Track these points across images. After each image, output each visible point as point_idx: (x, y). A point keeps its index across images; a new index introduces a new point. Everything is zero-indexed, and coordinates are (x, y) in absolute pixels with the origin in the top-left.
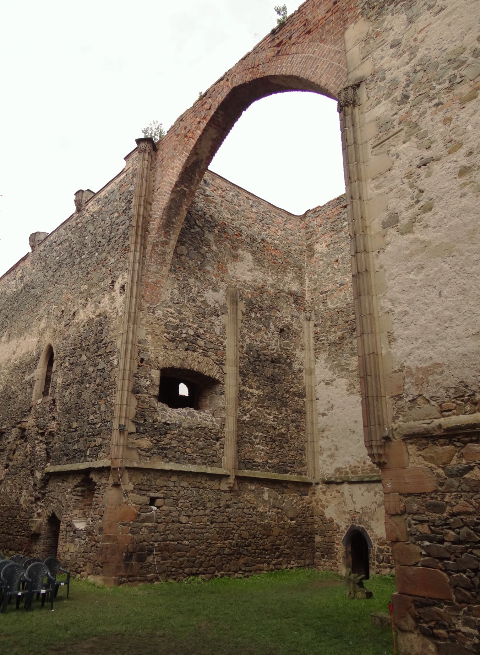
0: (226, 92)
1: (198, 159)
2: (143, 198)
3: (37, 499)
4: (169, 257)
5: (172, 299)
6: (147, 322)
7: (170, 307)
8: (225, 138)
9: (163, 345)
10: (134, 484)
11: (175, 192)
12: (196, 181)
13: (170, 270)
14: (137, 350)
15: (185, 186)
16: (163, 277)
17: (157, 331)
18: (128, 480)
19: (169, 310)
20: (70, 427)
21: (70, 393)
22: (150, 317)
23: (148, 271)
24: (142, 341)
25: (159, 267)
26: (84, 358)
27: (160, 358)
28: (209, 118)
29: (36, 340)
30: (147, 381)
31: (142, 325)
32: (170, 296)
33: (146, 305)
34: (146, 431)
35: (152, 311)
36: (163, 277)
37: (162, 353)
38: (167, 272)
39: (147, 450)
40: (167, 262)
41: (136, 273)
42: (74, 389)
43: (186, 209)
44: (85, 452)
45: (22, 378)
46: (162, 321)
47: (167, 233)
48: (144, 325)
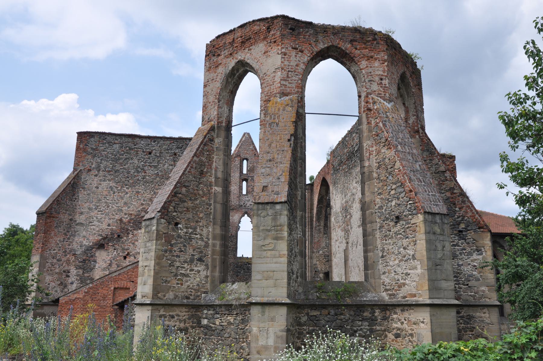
4: (322, 230)
7: (325, 248)
16: (321, 238)
19: (325, 250)
22: (317, 255)
33: (315, 251)
36: (321, 238)
47: (319, 222)
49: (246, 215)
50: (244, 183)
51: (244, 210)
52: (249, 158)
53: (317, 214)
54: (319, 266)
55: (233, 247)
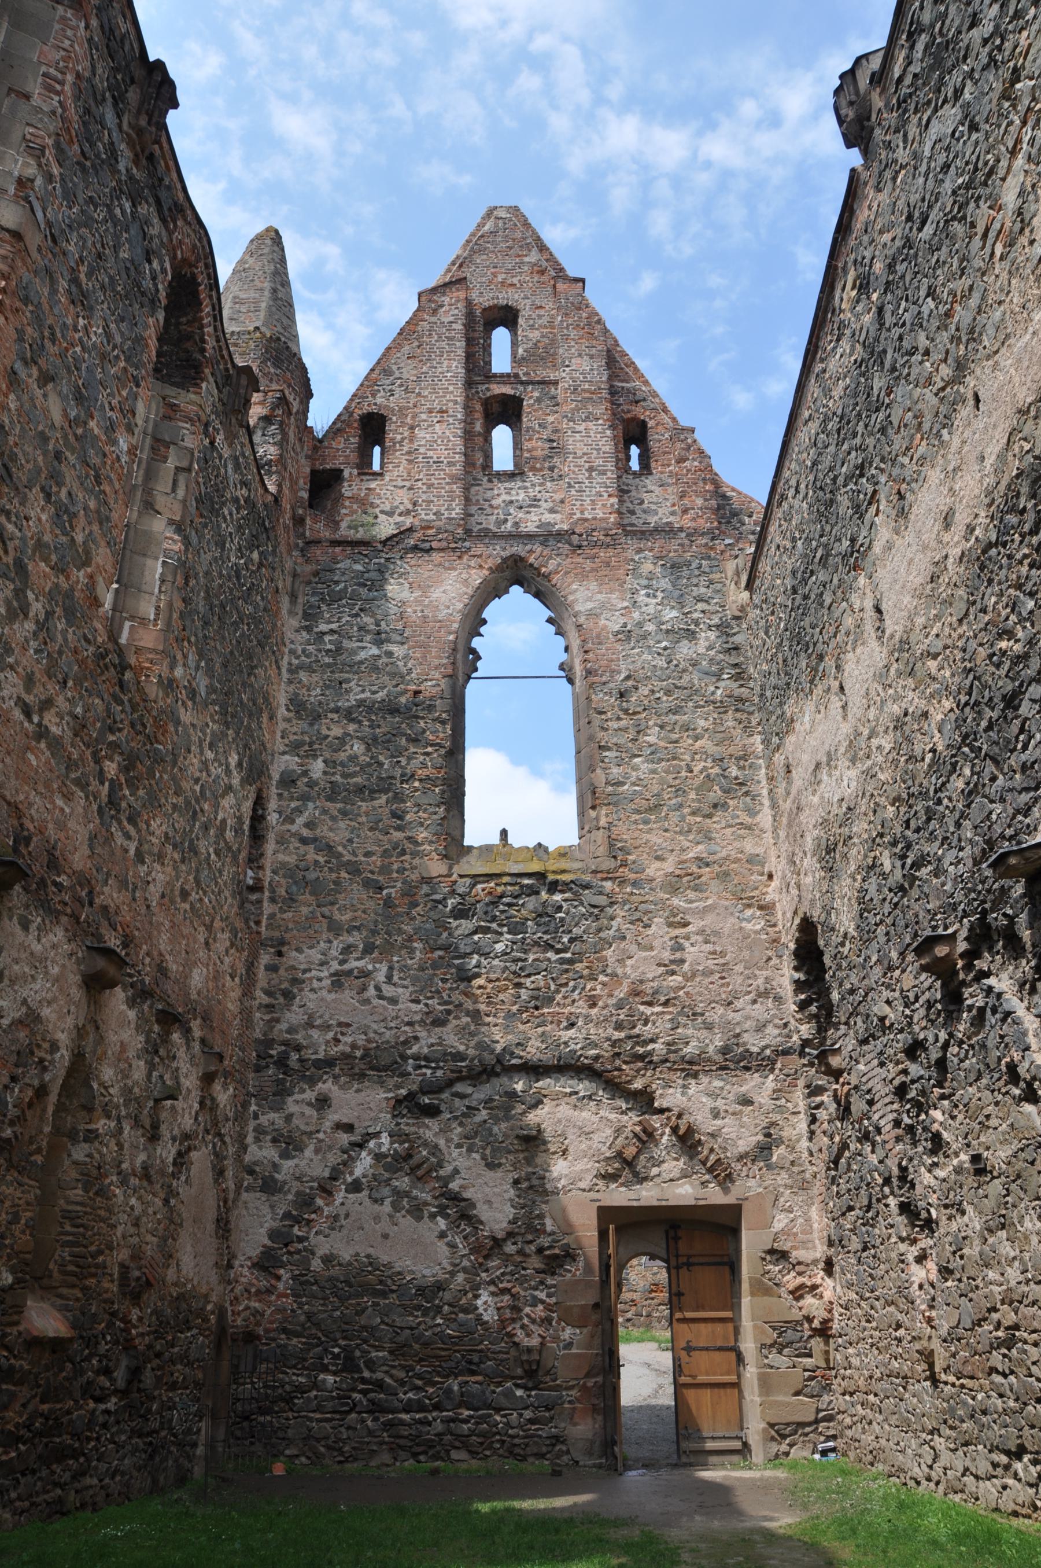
51: (498, 552)
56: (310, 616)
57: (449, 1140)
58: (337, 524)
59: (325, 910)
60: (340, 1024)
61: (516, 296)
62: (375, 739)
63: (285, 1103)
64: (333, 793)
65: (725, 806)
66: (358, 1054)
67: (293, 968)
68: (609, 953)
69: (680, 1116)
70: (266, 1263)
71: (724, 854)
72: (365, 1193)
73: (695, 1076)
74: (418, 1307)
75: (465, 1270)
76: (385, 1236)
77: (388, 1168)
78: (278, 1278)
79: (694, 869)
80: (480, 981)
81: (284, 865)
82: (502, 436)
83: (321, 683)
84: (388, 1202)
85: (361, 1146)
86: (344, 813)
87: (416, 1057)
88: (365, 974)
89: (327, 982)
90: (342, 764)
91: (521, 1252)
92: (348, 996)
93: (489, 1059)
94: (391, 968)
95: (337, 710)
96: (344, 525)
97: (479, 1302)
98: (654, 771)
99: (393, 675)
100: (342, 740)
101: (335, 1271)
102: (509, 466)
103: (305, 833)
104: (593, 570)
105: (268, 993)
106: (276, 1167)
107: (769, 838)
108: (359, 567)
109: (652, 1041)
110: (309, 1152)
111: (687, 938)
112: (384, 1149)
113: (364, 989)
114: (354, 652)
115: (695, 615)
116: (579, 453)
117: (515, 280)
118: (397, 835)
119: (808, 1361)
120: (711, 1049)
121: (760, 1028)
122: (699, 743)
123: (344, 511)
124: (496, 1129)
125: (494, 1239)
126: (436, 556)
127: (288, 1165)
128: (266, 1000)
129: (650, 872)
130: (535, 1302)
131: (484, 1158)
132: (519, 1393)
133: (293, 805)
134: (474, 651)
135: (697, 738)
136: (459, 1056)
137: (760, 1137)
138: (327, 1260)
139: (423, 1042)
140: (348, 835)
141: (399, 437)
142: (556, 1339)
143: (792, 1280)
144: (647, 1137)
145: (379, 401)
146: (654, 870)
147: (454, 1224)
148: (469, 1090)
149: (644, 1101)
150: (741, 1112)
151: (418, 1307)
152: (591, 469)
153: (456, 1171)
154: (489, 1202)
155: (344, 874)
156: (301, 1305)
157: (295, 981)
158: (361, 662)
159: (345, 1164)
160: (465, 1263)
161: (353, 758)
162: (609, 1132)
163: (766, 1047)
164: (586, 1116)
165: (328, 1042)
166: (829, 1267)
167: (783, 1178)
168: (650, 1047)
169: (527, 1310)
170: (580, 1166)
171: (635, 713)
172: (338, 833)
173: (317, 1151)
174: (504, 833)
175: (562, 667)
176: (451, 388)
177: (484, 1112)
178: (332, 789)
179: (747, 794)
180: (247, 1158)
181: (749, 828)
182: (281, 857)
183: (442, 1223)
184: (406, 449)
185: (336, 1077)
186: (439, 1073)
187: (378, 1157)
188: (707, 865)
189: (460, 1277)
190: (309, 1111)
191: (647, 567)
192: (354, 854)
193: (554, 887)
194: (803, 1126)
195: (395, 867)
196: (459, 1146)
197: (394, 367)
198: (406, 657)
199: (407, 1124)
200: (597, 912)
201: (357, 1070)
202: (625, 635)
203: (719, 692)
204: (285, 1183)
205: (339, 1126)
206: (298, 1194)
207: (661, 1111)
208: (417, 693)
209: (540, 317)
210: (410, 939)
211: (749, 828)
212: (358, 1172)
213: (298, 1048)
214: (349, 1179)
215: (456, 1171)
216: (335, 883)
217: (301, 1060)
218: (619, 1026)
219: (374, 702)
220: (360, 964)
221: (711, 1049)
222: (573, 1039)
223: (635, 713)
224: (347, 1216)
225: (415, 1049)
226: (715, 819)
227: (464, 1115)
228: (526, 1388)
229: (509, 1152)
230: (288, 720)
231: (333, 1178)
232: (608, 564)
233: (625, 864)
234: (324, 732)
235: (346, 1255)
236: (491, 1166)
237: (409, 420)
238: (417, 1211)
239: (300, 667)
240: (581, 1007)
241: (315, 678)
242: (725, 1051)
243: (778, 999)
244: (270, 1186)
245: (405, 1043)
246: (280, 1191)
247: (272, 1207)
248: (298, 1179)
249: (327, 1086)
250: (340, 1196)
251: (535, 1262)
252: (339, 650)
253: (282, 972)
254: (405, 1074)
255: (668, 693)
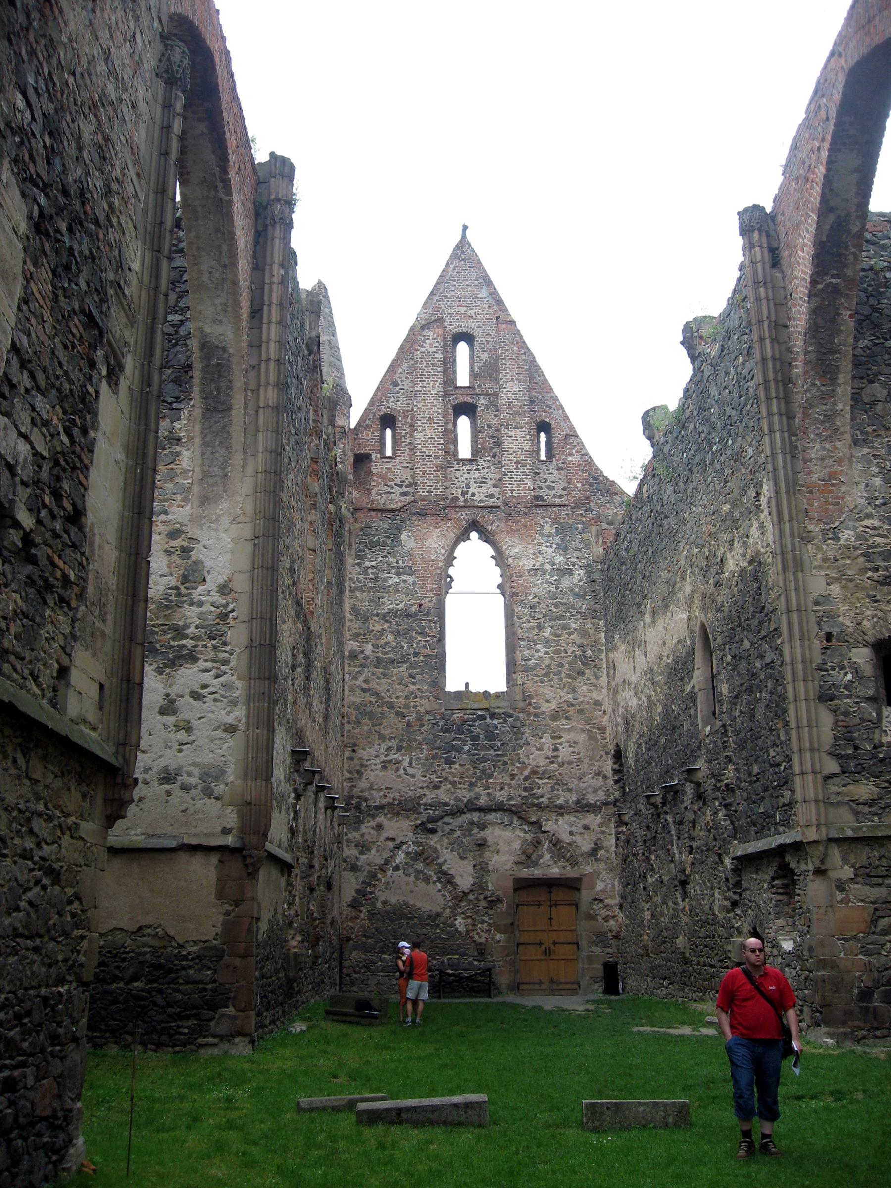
0: (841, 79)
1: (839, 217)
2: (766, 324)
3: (735, 904)
4: (844, 422)
5: (870, 500)
6: (825, 560)
7: (869, 516)
8: (877, 156)
9: (868, 596)
10: (853, 867)
11: (815, 295)
12: (851, 258)
13: (856, 443)
14: (813, 619)
15: (833, 276)
17: (849, 573)
18: (840, 862)
19: (867, 522)
20: (750, 774)
21: (741, 712)
22: (830, 549)
23: (805, 461)
24: (821, 600)
25: (827, 446)
26: (747, 644)
27: (865, 622)
28: (829, 137)
29: (684, 616)
30: (846, 674)
31: (815, 568)
32: (865, 494)
34: (861, 769)
35: (831, 535)
36: (839, 462)
37: (869, 613)
38: (847, 451)
39: (871, 803)
40: (842, 429)
41: (781, 473)
42: (744, 703)
43: (851, 316)
44: (774, 816)
45: (682, 691)
46: (856, 549)
48: (820, 567)
49: (474, 535)
50: (464, 423)
51: (465, 516)
52: (478, 334)
53: (814, 330)
54: (843, 608)
55: (428, 651)
56: (360, 556)
57: (442, 846)
58: (370, 490)
59: (376, 728)
60: (387, 788)
61: (473, 326)
62: (399, 632)
63: (360, 827)
64: (378, 662)
65: (583, 674)
66: (396, 803)
67: (361, 758)
68: (521, 752)
69: (554, 835)
70: (355, 905)
71: (581, 700)
72: (402, 871)
73: (562, 815)
74: (428, 925)
75: (450, 907)
76: (412, 892)
77: (411, 859)
78: (361, 911)
79: (566, 707)
80: (457, 766)
81: (354, 703)
82: (464, 423)
83: (368, 599)
84: (413, 875)
85: (398, 847)
86: (384, 675)
87: (425, 805)
88: (398, 762)
89: (379, 766)
90: (382, 647)
91: (476, 899)
92: (390, 774)
93: (461, 805)
94: (411, 759)
95: (377, 615)
96: (374, 492)
97: (457, 922)
98: (547, 653)
99: (407, 594)
100: (382, 632)
101: (388, 908)
102: (469, 456)
103: (364, 686)
104: (518, 530)
105: (350, 772)
106: (357, 859)
107: (605, 691)
108: (386, 526)
109: (542, 797)
110: (373, 852)
111: (561, 744)
112: (410, 850)
113: (398, 770)
114: (385, 580)
115: (573, 560)
116: (511, 452)
117: (472, 312)
118: (412, 687)
119: (609, 950)
120: (571, 801)
121: (595, 791)
122: (572, 636)
123: (373, 483)
124: (464, 840)
125: (464, 893)
126: (429, 518)
127: (363, 858)
128: (349, 775)
129: (543, 709)
130: (483, 922)
131: (459, 854)
132: (476, 963)
133: (357, 669)
134: (450, 577)
135: (570, 634)
136: (446, 804)
137: (593, 846)
138: (384, 903)
139: (428, 797)
140: (387, 687)
141: (404, 432)
142: (493, 939)
143: (604, 913)
144: (538, 843)
145: (391, 405)
146: (545, 708)
147: (445, 886)
148: (451, 821)
149: (537, 824)
150: (583, 833)
151: (428, 925)
152: (517, 463)
153: (445, 861)
154: (462, 876)
155: (385, 709)
156: (372, 924)
157: (362, 765)
158: (390, 586)
159: (391, 857)
160: (450, 904)
161: (387, 643)
162: (519, 842)
163: (598, 801)
164: (507, 834)
165: (381, 797)
166: (621, 907)
167: (602, 866)
168: (541, 800)
169: (480, 925)
170: (505, 858)
171: (538, 619)
172: (381, 686)
173: (378, 851)
174: (467, 684)
175: (499, 586)
176: (435, 402)
177: (459, 832)
178: (377, 661)
179: (595, 666)
180: (344, 855)
181: (595, 685)
182: (353, 699)
183: (439, 885)
184: (408, 441)
185: (385, 815)
186: (437, 812)
187: (408, 854)
188: (573, 705)
189: (448, 911)
190: (372, 831)
191: (547, 529)
192: (390, 697)
193: (493, 716)
194: (613, 841)
195: (412, 705)
196: (447, 848)
197: (399, 380)
198: (414, 583)
199: (421, 838)
200: (517, 730)
201: (395, 811)
202: (534, 571)
203: (584, 607)
204: (362, 866)
205: (387, 839)
206: (369, 871)
207: (545, 832)
208: (421, 605)
209: (488, 342)
210: (420, 744)
211: (595, 685)
212: (398, 861)
213: (366, 800)
214: (394, 865)
215: (445, 861)
216: (381, 713)
217: (368, 806)
218: (525, 789)
219: (398, 610)
220: (396, 756)
221: (571, 801)
222: (501, 796)
223: (538, 619)
224: (393, 882)
225: (424, 801)
226: (578, 680)
227: (449, 833)
228: (479, 961)
229: (471, 851)
230: (351, 620)
231: (386, 864)
232: (525, 527)
233: (530, 704)
234: (372, 628)
235: (393, 900)
236: (463, 858)
237: (409, 420)
238: (427, 880)
239: (356, 588)
240: (507, 779)
241: (365, 595)
242: (577, 802)
243: (605, 777)
244: (354, 868)
245: (420, 797)
246: (360, 870)
247: (356, 878)
248: (369, 865)
249: (381, 819)
250: (389, 873)
251: (483, 904)
252: (376, 579)
253: (356, 761)
254: (420, 813)
255: (556, 606)
